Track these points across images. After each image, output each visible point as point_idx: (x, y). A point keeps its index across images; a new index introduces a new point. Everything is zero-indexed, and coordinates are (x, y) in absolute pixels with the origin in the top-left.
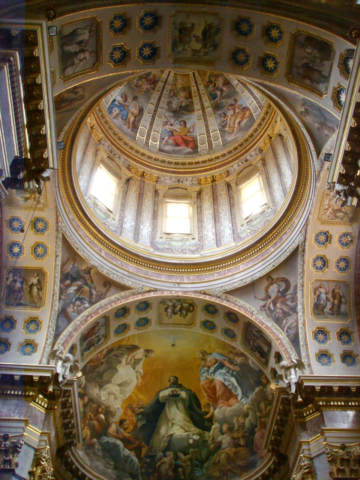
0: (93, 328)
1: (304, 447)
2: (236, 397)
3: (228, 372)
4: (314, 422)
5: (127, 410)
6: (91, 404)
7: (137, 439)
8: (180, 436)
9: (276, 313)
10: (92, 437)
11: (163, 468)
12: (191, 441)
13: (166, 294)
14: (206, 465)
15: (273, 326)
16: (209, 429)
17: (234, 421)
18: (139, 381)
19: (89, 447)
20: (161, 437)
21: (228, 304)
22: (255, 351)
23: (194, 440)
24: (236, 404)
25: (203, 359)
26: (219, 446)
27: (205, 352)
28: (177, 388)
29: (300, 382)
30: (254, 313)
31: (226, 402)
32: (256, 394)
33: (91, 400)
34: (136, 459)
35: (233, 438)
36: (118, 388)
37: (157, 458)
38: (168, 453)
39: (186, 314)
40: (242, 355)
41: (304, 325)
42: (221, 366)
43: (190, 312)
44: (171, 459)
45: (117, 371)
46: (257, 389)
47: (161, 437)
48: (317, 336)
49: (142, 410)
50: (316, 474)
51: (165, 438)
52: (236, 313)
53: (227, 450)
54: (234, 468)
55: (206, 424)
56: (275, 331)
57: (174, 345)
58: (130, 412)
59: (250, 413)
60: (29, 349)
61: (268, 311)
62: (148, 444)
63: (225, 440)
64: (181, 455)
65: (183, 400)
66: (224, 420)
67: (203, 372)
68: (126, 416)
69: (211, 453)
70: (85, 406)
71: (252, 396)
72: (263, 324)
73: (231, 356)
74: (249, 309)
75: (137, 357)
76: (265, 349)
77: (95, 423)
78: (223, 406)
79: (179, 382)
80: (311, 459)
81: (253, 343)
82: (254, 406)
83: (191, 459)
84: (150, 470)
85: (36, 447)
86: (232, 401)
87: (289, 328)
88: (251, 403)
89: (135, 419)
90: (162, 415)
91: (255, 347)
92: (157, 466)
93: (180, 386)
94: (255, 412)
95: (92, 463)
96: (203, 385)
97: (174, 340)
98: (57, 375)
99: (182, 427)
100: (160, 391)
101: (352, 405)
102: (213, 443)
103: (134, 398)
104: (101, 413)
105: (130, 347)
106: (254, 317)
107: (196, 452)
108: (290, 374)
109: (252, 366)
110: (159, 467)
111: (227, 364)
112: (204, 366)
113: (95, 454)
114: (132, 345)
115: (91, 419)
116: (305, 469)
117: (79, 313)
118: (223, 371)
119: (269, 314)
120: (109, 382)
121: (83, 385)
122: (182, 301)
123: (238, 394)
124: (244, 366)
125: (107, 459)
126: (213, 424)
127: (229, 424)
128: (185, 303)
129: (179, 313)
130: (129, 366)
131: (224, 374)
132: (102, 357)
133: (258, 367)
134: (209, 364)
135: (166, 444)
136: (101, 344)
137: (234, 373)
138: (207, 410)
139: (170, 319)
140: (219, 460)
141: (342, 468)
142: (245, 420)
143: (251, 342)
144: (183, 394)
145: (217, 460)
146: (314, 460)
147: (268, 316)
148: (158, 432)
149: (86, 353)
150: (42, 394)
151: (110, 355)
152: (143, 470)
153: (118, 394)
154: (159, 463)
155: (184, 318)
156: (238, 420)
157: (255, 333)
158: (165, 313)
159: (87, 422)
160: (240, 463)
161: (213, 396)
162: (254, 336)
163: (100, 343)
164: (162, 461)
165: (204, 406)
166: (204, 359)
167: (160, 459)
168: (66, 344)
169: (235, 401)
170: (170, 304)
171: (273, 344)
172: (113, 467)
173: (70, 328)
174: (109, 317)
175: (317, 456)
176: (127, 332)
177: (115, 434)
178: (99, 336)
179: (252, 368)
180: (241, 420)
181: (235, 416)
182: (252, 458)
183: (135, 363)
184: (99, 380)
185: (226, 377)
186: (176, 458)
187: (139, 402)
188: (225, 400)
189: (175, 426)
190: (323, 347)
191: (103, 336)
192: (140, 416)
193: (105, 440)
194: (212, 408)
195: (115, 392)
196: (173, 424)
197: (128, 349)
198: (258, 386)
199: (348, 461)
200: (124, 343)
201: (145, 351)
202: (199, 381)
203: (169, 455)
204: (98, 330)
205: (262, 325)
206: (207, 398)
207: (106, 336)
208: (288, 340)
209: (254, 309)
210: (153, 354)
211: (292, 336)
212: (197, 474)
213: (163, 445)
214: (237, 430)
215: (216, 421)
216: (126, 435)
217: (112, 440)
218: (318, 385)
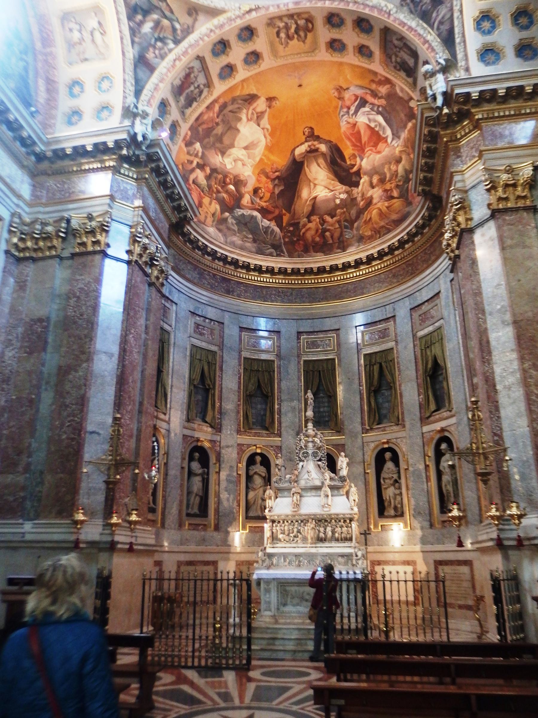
0: (188, 76)
1: (457, 178)
2: (385, 140)
3: (372, 109)
4: (472, 145)
5: (260, 177)
6: (215, 175)
7: (276, 207)
8: (324, 198)
9: (422, 6)
10: (222, 212)
11: (309, 235)
12: (338, 201)
13: (272, 10)
14: (356, 225)
15: (418, 25)
16: (357, 185)
17: (386, 170)
18: (268, 140)
19: (221, 222)
20: (303, 201)
21: (356, 6)
22: (399, 70)
23: (342, 200)
24: (387, 150)
25: (339, 98)
26: (369, 202)
27: (341, 87)
28: (314, 141)
29: (449, 91)
30: (391, 12)
31: (374, 149)
32: (409, 131)
33: (214, 171)
34: (277, 229)
35: (386, 191)
36: (244, 152)
37: (301, 225)
38: (313, 218)
39: (306, 36)
40: (387, 81)
41: (461, 12)
42: (363, 103)
43: (310, 31)
44: (317, 224)
45: (238, 131)
46: (410, 125)
47: (303, 201)
48: (480, 25)
49: (277, 174)
50: (471, 210)
51: (308, 202)
52: (368, 18)
53: (379, 205)
54: (387, 224)
55: (354, 179)
56: (421, 32)
57: (300, 86)
58: (264, 179)
59: (404, 157)
60: (105, 113)
61: (411, 5)
62: (289, 211)
63: (376, 193)
64: (328, 218)
65: (323, 155)
66: (374, 171)
67: (343, 116)
68: (260, 183)
69: (360, 212)
70: (208, 178)
71: (404, 135)
72: (404, 24)
73: (374, 86)
74: (385, 9)
75: (259, 110)
76: (411, 62)
77: (225, 195)
78: (371, 154)
79: (316, 134)
80: (466, 192)
81: (396, 60)
82: (408, 147)
83: (339, 222)
84: (295, 239)
85: (130, 224)
86: (381, 146)
87: (441, 23)
88: (403, 144)
89: (271, 186)
90: (302, 176)
91: (399, 63)
92: (301, 233)
93: (318, 138)
94: (409, 154)
95: (226, 238)
96: (345, 133)
97: (300, 78)
98: (136, 134)
99: (326, 187)
100: (294, 150)
101: (526, 114)
102: (362, 200)
103: (266, 161)
104: (230, 184)
105: (248, 97)
106: (392, 18)
107: (344, 212)
108: (436, 82)
109: (401, 94)
110: (304, 234)
111: (370, 99)
112: (342, 107)
113: (229, 229)
114: (249, 95)
115: (218, 192)
116: (456, 205)
117: (163, 57)
118: (367, 109)
119: (413, 10)
120: (232, 146)
121: (200, 154)
122: (295, 17)
123: (387, 137)
124: (391, 96)
125: (244, 233)
126: (361, 178)
127: (379, 175)
128: (300, 19)
129: (296, 36)
130: (252, 123)
131: (368, 114)
132: (215, 115)
133: (408, 94)
134: (348, 103)
135: (310, 208)
136: (205, 98)
137: (380, 109)
138: (353, 163)
139: (286, 49)
140: (371, 218)
141: (505, 196)
142: (397, 166)
143: (393, 60)
144: (323, 148)
145: (368, 219)
146: (470, 193)
147: (411, 12)
148: (300, 196)
149: (188, 111)
150: (127, 163)
151: (225, 111)
152: (287, 240)
153: (246, 159)
154: (303, 230)
155: (304, 42)
156: (390, 169)
157: (396, 42)
158: (277, 39)
159: (214, 195)
160: (394, 217)
161: (358, 144)
162: (396, 47)
163: (203, 96)
164: (308, 227)
165: (349, 158)
166: (341, 98)
167: (304, 226)
168: (152, 101)
169: (385, 145)
170: (282, 25)
171: (419, 52)
172: (251, 240)
173: (154, 79)
174: (204, 57)
175: (473, 187)
176: (235, 76)
177: (250, 205)
178: (199, 86)
179: (401, 98)
180: (393, 168)
181: (386, 164)
182: (407, 209)
183: (258, 117)
184: (218, 145)
185: (371, 117)
186: (323, 222)
187: (273, 165)
188: (373, 146)
189: (317, 186)
190: (489, 39)
191: (204, 85)
192: (277, 182)
193: (239, 213)
194: (358, 159)
195: (242, 157)
196: (315, 185)
197: (245, 100)
198: (410, 121)
199: (514, 186)
200: (238, 93)
201: (267, 99)
202: (339, 127)
203: (314, 220)
204: (196, 77)
205: (403, 27)
206: (351, 148)
207: (209, 85)
208: (439, 40)
209: (390, 6)
210: (277, 102)
211: (445, 33)
212: (347, 237)
213: (307, 209)
214: (389, 181)
215: (365, 174)
216: (264, 204)
217: (247, 212)
218: (475, 91)
